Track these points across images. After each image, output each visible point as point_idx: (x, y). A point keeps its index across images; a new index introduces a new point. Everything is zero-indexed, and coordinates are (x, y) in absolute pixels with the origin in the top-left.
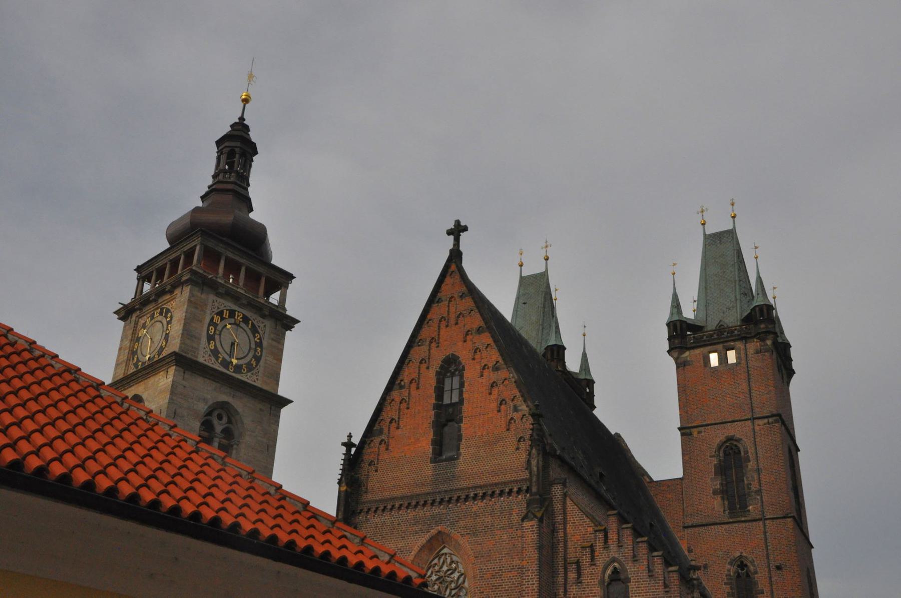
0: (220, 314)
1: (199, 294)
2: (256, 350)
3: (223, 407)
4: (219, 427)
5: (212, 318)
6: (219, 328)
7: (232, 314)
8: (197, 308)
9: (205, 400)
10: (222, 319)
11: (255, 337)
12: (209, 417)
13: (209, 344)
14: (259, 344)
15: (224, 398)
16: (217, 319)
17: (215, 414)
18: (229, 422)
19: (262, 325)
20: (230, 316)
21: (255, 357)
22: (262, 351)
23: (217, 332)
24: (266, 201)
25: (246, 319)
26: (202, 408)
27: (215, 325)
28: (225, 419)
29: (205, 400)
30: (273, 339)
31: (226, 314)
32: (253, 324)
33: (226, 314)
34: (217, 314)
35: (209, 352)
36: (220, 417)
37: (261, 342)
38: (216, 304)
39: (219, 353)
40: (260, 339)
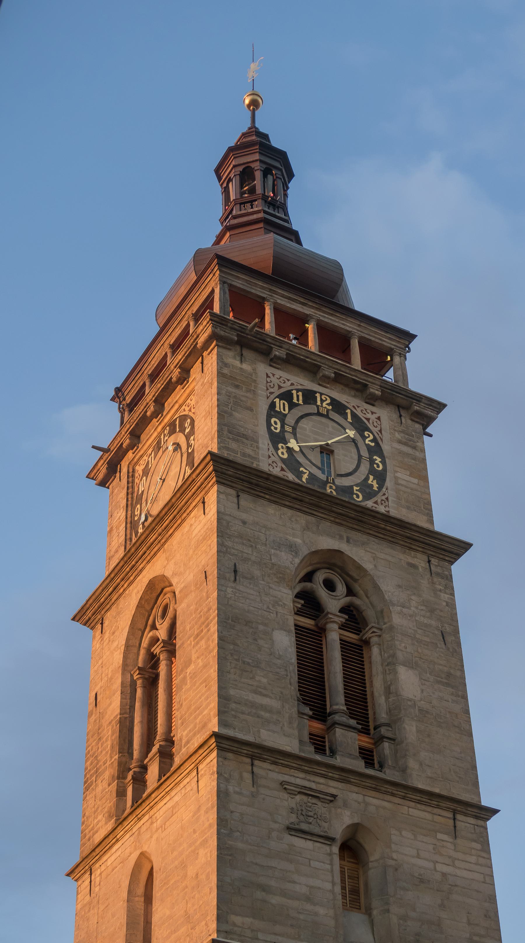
0: (287, 396)
1: (237, 363)
2: (372, 462)
3: (332, 562)
4: (333, 603)
5: (272, 405)
6: (290, 420)
7: (309, 397)
8: (237, 387)
9: (292, 548)
10: (292, 406)
11: (364, 438)
12: (308, 585)
13: (277, 449)
14: (376, 449)
15: (326, 543)
16: (281, 405)
17: (320, 576)
18: (350, 592)
19: (373, 417)
20: (305, 402)
21: (372, 471)
22: (384, 462)
23: (288, 428)
24: (331, 220)
25: (339, 407)
26: (290, 563)
27: (282, 417)
28: (341, 588)
29: (292, 548)
30: (400, 442)
31: (298, 398)
32: (352, 412)
33: (298, 398)
34: (281, 397)
35: (280, 464)
36: (330, 585)
37: (377, 444)
38: (274, 380)
39: (300, 465)
40: (374, 440)
